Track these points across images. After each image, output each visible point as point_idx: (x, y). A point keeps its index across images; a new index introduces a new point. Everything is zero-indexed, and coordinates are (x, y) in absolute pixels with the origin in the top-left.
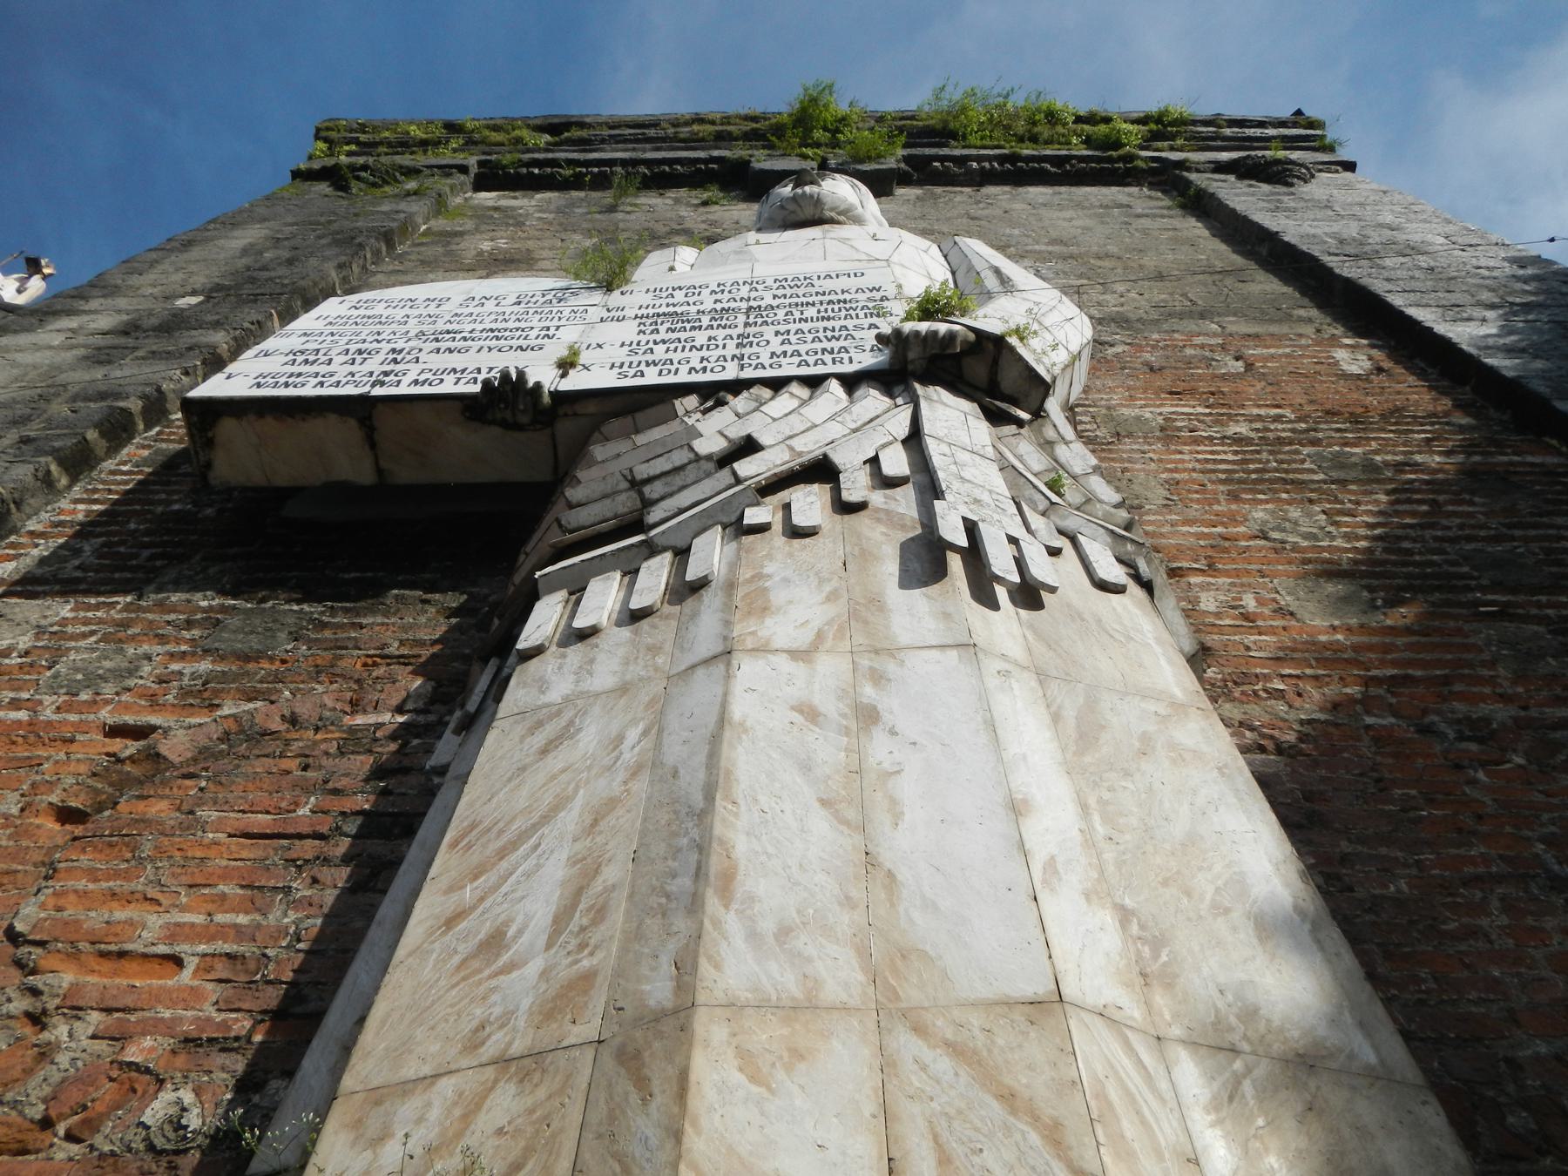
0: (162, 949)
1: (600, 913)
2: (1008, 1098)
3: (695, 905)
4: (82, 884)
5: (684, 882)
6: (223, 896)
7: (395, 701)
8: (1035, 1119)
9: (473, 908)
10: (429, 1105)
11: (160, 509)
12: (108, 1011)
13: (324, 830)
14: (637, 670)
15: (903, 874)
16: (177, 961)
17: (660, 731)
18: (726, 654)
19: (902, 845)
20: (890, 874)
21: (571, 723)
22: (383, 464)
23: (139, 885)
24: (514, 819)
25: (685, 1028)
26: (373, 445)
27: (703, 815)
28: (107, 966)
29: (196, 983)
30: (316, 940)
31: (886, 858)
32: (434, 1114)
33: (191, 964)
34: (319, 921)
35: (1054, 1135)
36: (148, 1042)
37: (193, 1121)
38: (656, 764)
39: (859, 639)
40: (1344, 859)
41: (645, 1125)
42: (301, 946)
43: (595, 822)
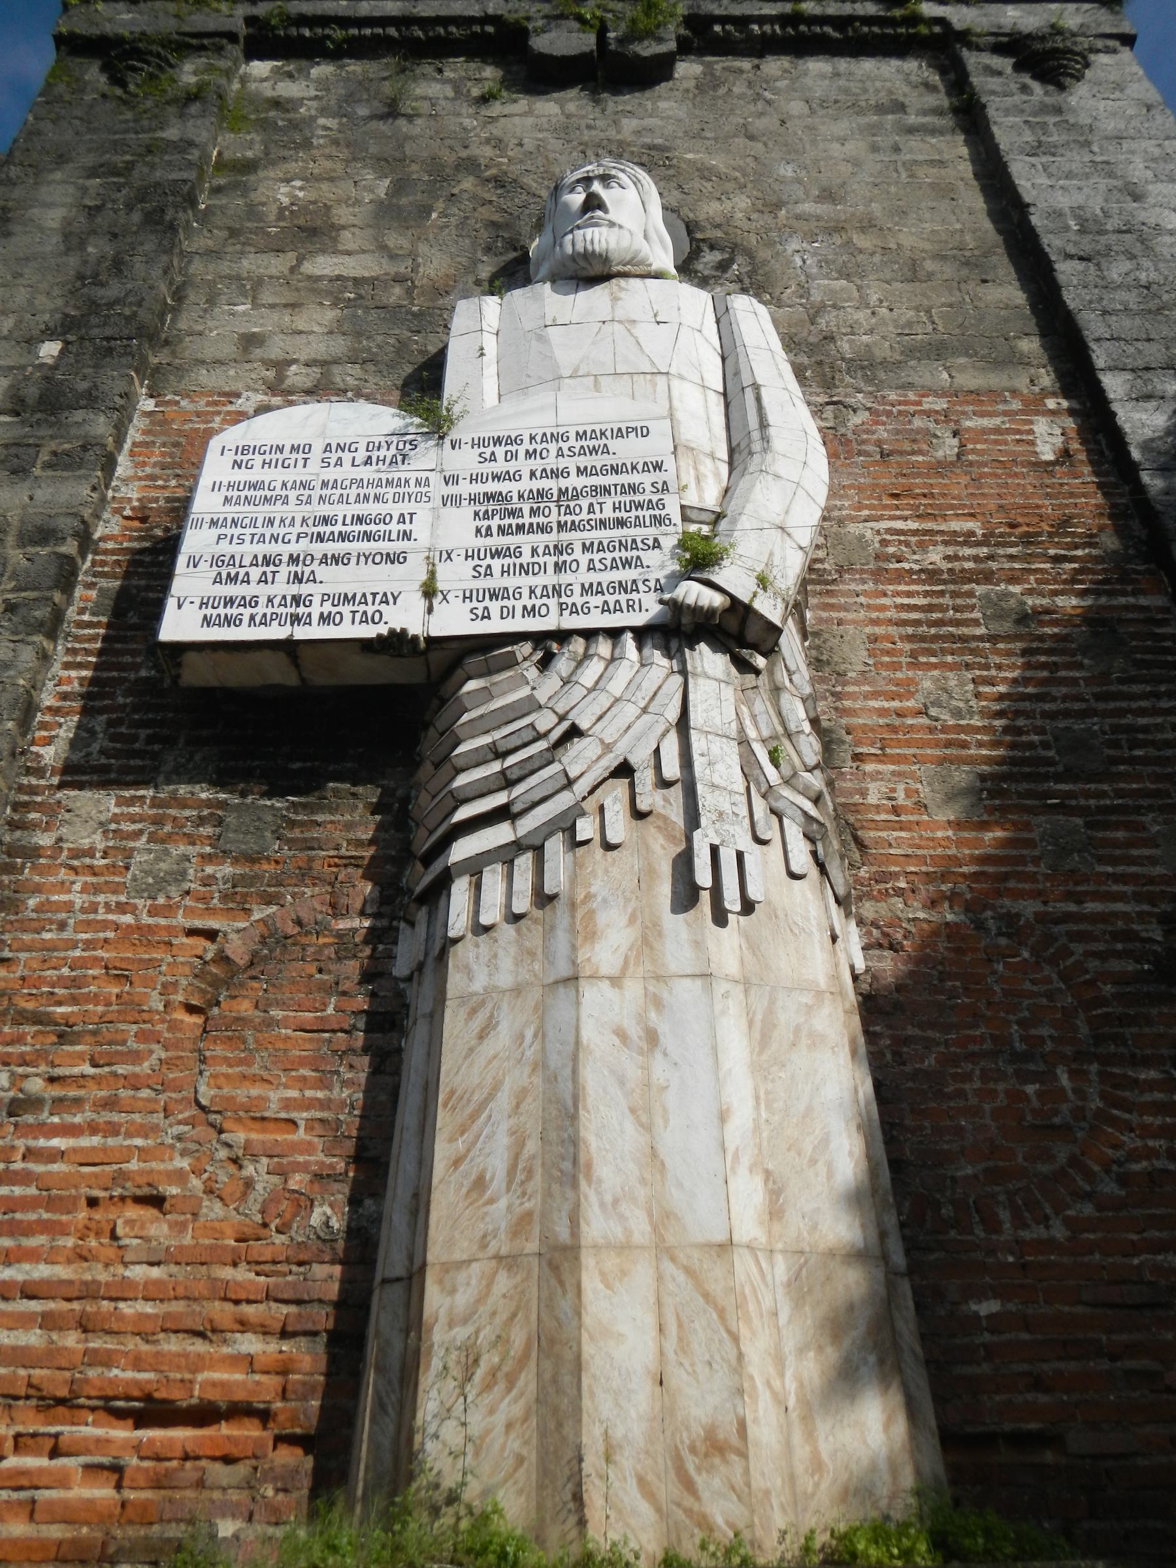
0: (283, 1115)
1: (530, 1173)
2: (706, 1296)
3: (575, 1185)
4: (224, 1069)
5: (567, 1165)
6: (304, 1078)
7: (358, 905)
8: (716, 1307)
9: (465, 1156)
10: (470, 1277)
11: (132, 676)
12: (271, 1156)
13: (347, 1027)
14: (525, 975)
15: (668, 1163)
16: (293, 1123)
17: (544, 1036)
18: (573, 980)
19: (669, 1140)
20: (663, 1164)
21: (492, 1016)
22: (305, 675)
23: (255, 1069)
24: (473, 1092)
25: (577, 1258)
26: (297, 666)
27: (574, 1117)
28: (257, 1125)
29: (308, 1138)
30: (364, 1108)
31: (663, 1152)
32: (474, 1282)
33: (302, 1124)
34: (361, 1095)
35: (722, 1313)
36: (297, 1177)
37: (335, 1224)
38: (545, 1066)
39: (649, 966)
40: (907, 1041)
41: (565, 1305)
42: (356, 1112)
43: (518, 1106)
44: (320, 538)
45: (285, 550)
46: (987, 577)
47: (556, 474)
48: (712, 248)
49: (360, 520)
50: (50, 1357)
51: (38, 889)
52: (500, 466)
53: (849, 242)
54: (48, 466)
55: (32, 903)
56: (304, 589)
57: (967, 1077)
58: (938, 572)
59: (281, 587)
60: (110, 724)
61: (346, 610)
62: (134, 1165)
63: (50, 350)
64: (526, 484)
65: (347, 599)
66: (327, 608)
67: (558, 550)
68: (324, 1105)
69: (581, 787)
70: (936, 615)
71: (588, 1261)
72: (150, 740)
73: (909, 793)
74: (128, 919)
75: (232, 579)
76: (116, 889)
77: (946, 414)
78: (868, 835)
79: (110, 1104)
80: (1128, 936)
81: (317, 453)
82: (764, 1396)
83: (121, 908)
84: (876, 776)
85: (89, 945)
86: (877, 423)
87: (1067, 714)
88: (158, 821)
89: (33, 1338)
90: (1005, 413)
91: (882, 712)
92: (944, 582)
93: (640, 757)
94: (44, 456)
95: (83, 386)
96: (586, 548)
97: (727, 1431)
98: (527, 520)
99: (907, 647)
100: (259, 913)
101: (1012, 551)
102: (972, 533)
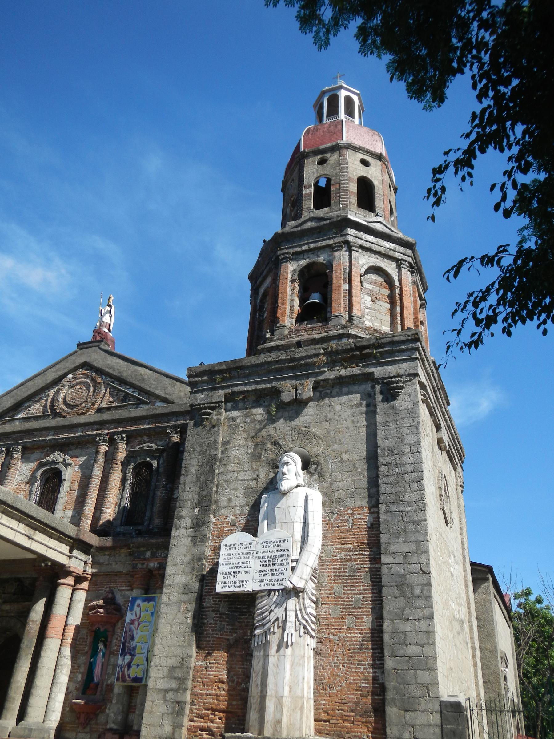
44: (238, 568)
45: (233, 570)
46: (350, 560)
47: (273, 551)
48: (314, 464)
49: (243, 563)
50: (213, 703)
51: (206, 630)
52: (264, 549)
53: (342, 459)
54: (199, 542)
55: (205, 633)
56: (236, 579)
57: (327, 666)
58: (343, 559)
59: (233, 579)
60: (213, 598)
61: (241, 584)
62: (221, 677)
63: (197, 510)
64: (269, 554)
65: (242, 582)
66: (239, 584)
67: (272, 570)
68: (244, 668)
69: (272, 622)
70: (339, 571)
71: (267, 698)
72: (219, 601)
73: (329, 612)
74: (217, 636)
75: (225, 577)
76: (216, 631)
77: (352, 514)
78: (321, 620)
79: (217, 667)
80: (357, 641)
81: (237, 546)
82: (285, 716)
83: (217, 634)
84: (324, 608)
85: (213, 641)
86: (339, 518)
87: (356, 594)
88: (220, 618)
89: (211, 701)
90: (363, 514)
91: (327, 594)
92: (342, 562)
93: (280, 616)
94: (198, 539)
95: (203, 520)
96: (276, 570)
97: (280, 720)
98: (268, 563)
99: (333, 578)
100: (234, 635)
101: (356, 553)
102: (350, 548)
